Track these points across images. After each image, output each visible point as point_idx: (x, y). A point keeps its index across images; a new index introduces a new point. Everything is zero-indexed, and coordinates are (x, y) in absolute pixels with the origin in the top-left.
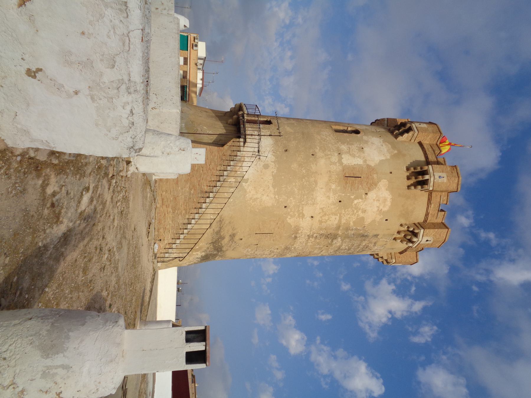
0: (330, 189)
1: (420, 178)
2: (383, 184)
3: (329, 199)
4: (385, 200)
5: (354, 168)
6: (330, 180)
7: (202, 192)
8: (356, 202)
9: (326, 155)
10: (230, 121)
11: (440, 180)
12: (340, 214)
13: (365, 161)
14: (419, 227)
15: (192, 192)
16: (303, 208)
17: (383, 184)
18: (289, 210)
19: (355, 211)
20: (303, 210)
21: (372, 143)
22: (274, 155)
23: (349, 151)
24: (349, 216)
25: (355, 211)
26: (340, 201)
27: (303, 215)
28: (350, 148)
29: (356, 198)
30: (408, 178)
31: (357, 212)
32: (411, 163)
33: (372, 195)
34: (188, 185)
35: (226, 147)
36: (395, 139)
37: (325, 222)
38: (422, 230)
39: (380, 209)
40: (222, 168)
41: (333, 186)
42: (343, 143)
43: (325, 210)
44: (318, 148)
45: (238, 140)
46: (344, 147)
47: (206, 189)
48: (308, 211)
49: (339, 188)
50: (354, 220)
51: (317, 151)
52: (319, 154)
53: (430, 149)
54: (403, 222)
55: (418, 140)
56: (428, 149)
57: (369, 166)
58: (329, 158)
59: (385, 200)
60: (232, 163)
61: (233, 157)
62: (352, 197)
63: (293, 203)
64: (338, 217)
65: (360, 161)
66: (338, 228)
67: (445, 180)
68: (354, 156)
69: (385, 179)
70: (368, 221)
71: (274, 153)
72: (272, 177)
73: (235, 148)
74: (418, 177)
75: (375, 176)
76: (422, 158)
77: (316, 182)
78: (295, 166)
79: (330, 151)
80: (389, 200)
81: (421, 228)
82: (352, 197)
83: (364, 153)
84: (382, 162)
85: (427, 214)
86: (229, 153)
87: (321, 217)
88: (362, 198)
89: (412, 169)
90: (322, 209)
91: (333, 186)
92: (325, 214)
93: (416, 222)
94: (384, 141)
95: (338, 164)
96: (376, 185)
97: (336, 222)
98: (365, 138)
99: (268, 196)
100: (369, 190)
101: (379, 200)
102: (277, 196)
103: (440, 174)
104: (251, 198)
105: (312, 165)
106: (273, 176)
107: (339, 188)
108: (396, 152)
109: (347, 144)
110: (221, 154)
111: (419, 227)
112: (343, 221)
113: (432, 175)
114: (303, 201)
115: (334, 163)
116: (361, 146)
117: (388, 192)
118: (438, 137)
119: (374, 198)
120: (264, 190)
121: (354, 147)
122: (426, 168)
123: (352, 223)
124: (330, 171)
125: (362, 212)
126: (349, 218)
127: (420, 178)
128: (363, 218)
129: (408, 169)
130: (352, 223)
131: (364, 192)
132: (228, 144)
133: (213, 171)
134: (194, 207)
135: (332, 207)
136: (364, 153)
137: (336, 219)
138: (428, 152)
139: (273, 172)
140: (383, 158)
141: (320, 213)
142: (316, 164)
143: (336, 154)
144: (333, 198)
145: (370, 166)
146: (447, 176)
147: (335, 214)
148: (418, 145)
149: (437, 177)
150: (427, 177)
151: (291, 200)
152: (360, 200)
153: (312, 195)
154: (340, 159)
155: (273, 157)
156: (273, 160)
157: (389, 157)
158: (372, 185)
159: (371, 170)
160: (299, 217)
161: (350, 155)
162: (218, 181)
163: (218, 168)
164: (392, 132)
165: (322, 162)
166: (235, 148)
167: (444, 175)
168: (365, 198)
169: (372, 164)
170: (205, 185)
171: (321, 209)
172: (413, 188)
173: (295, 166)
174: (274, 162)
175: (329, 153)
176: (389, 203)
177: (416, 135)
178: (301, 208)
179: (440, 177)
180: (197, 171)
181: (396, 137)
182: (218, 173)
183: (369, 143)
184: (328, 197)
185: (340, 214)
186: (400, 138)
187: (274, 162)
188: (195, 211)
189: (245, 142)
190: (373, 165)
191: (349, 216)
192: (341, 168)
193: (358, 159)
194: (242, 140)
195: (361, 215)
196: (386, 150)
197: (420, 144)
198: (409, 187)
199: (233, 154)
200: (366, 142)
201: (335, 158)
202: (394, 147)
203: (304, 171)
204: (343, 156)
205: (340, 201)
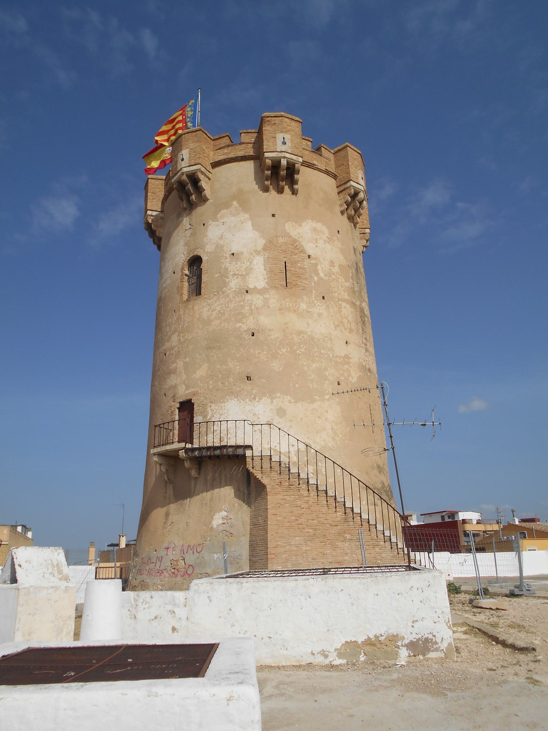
0: (308, 312)
1: (283, 173)
2: (293, 230)
3: (322, 314)
4: (315, 230)
5: (271, 272)
6: (295, 311)
7: (346, 520)
8: (322, 275)
9: (252, 313)
10: (193, 473)
11: (289, 144)
12: (340, 300)
13: (258, 253)
14: (346, 186)
15: (348, 536)
16: (337, 357)
17: (293, 230)
18: (342, 378)
19: (334, 277)
20: (340, 357)
21: (221, 238)
22: (260, 399)
23: (241, 275)
24: (340, 287)
25: (334, 277)
26: (323, 298)
27: (346, 356)
28: (234, 275)
29: (317, 274)
30: (280, 191)
31: (334, 275)
32: (256, 184)
33: (310, 249)
34: (340, 544)
35: (265, 481)
36: (208, 203)
37: (350, 324)
38: (352, 183)
39: (327, 239)
40: (304, 486)
41: (303, 306)
42: (226, 284)
43: (337, 323)
44: (238, 325)
45: (249, 460)
46: (234, 284)
47: (340, 513)
48: (341, 350)
49: (305, 298)
50: (343, 280)
51: (244, 327)
52: (250, 324)
53: (226, 151)
54: (338, 209)
55: (209, 167)
56: (226, 154)
57: (265, 249)
58: (257, 308)
59: (315, 230)
60: (294, 470)
61: (284, 469)
62: (316, 278)
63: (333, 371)
64: (344, 304)
65: (259, 263)
66: (353, 305)
67: (288, 137)
68: (249, 270)
69: (285, 227)
70: (340, 259)
71: (255, 398)
72: (299, 404)
73: (266, 465)
74: (279, 176)
75: (281, 240)
76: (250, 165)
77: (300, 333)
78: (276, 365)
79: (243, 307)
80: (314, 225)
81: (348, 184)
82: (316, 278)
83: (242, 253)
84: (255, 227)
85: (327, 172)
86: (275, 475)
87: (346, 329)
88: (316, 265)
89: (267, 183)
90: (336, 327)
91: (303, 306)
92: (342, 322)
93: (337, 191)
94: (215, 219)
95: (267, 296)
96: (295, 241)
97: (348, 306)
98: (209, 248)
99: (327, 412)
100: (303, 251)
101: (316, 240)
102: (327, 397)
103: (279, 141)
104: (334, 439)
105: (273, 337)
106: (296, 402)
107: (305, 298)
108: (235, 203)
109: (228, 278)
110: (280, 489)
111: (346, 186)
112: (346, 296)
113: (283, 154)
114: (329, 356)
115: (266, 300)
116: (228, 256)
117: (303, 224)
118: (205, 135)
119: (314, 246)
120: (319, 417)
121: (232, 267)
122: (269, 162)
123: (347, 284)
124: (280, 309)
125: (334, 266)
126: (342, 287)
127: (283, 173)
128: (341, 266)
129: (266, 190)
130: (347, 284)
131: (308, 260)
132: (259, 476)
133: (310, 503)
134: (369, 533)
135: (332, 310)
136: (242, 253)
137: (345, 307)
138: (232, 155)
139: (290, 402)
140: (249, 224)
141: (341, 330)
142: (270, 330)
143: (248, 297)
144: (320, 308)
145: (265, 245)
146: (282, 132)
147: (340, 307)
148: (217, 169)
149: (284, 148)
150: (284, 162)
151: (329, 374)
152: (319, 267)
153: (319, 340)
154: (256, 291)
155: (263, 401)
156: (269, 400)
157: (247, 216)
158: (295, 246)
159: (269, 246)
160: (348, 363)
161: (247, 274)
162: (326, 493)
163: (306, 493)
164: (191, 206)
165: (265, 320)
166: (266, 465)
167: (280, 137)
168: (315, 259)
169: (261, 243)
170: (335, 515)
171: (336, 328)
172: (296, 187)
173: (276, 365)
174: (272, 399)
175: (247, 308)
176: (319, 226)
177: (203, 169)
178: (338, 360)
179: (284, 143)
180: (315, 530)
181: (205, 200)
182: (313, 493)
183: (221, 242)
184: (320, 315)
185: (340, 300)
186: (207, 192)
187: (272, 399)
188: (373, 529)
189: (250, 447)
190: (264, 241)
191: (340, 287)
192: (273, 292)
193: (255, 262)
194: (248, 453)
195: (336, 269)
196: (233, 218)
197: (216, 164)
198: (294, 192)
199: (277, 468)
200: (219, 248)
201: (257, 300)
202: (227, 205)
203: (284, 350)
204: (251, 286)
205: (323, 298)
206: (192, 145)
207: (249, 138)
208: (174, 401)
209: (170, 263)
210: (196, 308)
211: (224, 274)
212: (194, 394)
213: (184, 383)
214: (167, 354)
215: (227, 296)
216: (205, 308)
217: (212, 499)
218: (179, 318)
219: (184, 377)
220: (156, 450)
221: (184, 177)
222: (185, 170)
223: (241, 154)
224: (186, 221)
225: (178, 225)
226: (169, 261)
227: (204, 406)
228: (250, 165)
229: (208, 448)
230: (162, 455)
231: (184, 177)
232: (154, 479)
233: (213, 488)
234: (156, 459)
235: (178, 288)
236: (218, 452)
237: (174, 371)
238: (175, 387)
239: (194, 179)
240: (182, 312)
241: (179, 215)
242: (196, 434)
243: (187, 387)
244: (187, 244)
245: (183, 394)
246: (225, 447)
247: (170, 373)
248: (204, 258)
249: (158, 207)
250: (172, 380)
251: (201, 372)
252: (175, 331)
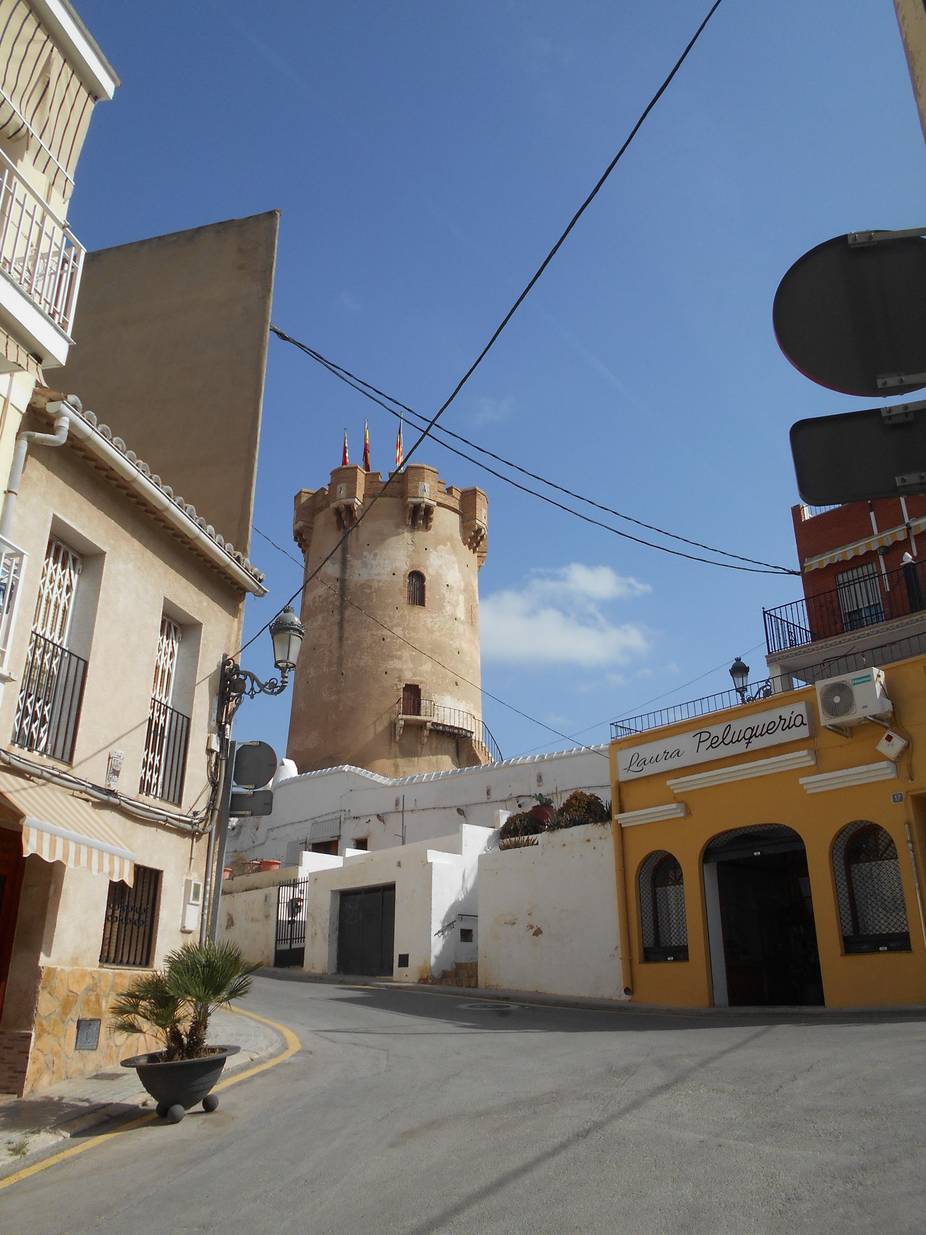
10: (426, 740)
46: (448, 609)
51: (455, 646)
52: (456, 644)
53: (443, 496)
65: (461, 598)
74: (473, 538)
84: (460, 572)
94: (435, 549)
121: (447, 595)
140: (456, 566)
143: (457, 623)
164: (414, 527)
165: (465, 646)
169: (463, 584)
181: (427, 528)
202: (445, 545)
204: (458, 616)
206: (432, 483)
207: (457, 494)
208: (400, 681)
209: (387, 562)
210: (421, 615)
211: (443, 598)
212: (421, 682)
213: (411, 670)
214: (388, 640)
215: (444, 617)
216: (423, 617)
217: (437, 762)
218: (403, 616)
219: (411, 666)
220: (405, 717)
221: (423, 506)
222: (426, 500)
223: (452, 505)
224: (407, 535)
225: (398, 534)
226: (384, 560)
227: (430, 694)
228: (456, 518)
229: (451, 727)
230: (405, 721)
231: (423, 506)
232: (371, 736)
233: (437, 754)
234: (402, 723)
235: (400, 589)
236: (456, 731)
237: (400, 658)
238: (401, 670)
239: (429, 510)
240: (406, 612)
241: (398, 526)
242: (422, 712)
243: (414, 675)
244: (409, 556)
245: (409, 677)
246: (462, 729)
247: (393, 657)
248: (427, 578)
249: (361, 498)
250: (396, 664)
251: (427, 667)
252: (398, 625)
